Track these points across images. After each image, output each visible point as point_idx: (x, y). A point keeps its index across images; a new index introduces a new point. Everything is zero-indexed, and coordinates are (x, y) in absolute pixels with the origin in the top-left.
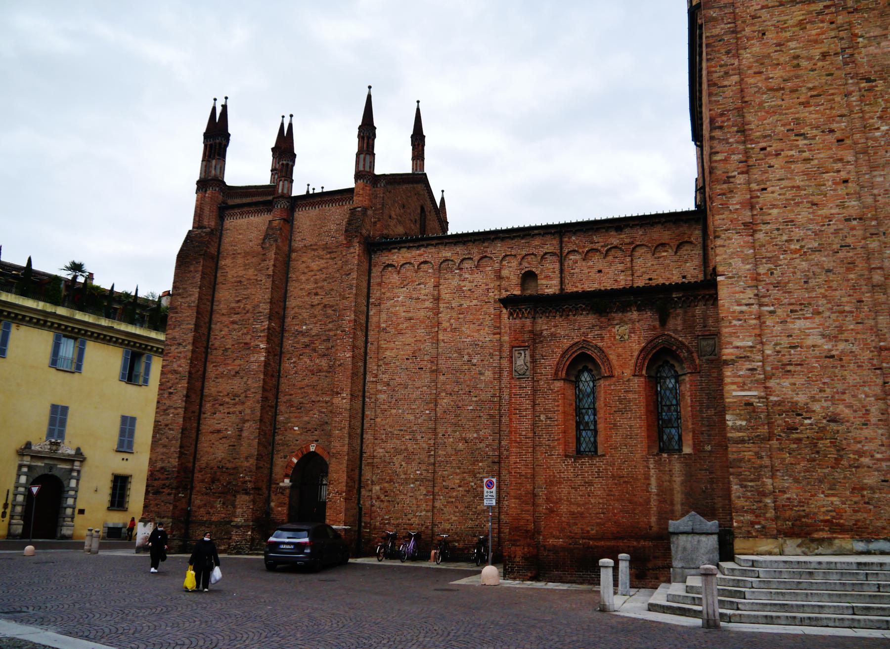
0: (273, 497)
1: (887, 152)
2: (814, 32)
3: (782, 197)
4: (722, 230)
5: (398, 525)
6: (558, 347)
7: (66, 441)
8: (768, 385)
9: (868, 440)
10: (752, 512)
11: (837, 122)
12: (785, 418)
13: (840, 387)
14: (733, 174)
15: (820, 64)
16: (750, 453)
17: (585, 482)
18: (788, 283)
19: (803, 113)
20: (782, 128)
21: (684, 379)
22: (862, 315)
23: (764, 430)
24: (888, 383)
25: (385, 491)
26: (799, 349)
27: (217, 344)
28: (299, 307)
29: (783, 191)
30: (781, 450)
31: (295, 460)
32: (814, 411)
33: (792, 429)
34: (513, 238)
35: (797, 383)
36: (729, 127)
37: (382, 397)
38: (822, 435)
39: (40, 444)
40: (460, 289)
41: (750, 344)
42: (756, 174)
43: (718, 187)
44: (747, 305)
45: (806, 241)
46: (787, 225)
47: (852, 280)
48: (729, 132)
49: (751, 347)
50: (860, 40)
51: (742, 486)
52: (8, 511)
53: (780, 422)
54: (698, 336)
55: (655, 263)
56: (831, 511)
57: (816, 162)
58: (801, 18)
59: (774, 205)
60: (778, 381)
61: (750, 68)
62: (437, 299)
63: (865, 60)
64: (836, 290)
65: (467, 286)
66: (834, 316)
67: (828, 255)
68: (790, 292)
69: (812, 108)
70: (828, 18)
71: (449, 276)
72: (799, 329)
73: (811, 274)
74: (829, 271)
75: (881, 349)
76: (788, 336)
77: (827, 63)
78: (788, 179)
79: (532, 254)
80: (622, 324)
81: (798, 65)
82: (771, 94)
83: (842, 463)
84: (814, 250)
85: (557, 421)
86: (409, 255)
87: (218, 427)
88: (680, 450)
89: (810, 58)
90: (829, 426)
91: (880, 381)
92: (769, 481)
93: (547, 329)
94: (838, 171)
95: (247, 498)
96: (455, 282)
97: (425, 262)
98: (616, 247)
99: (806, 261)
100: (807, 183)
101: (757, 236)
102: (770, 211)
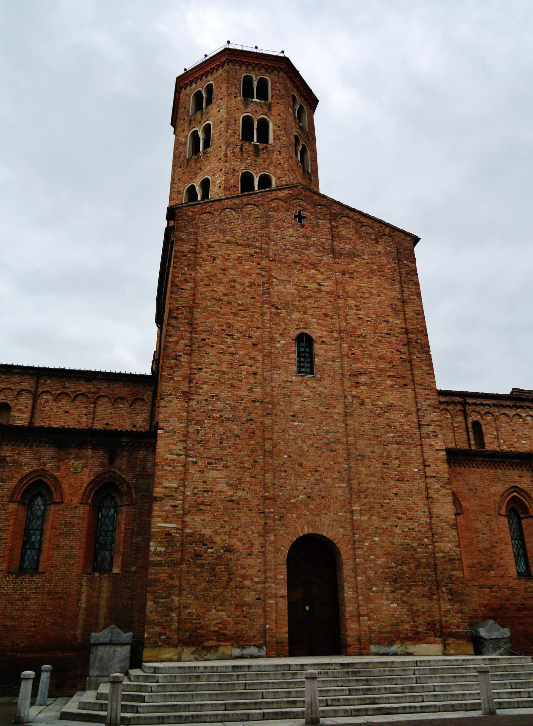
1: (282, 358)
2: (247, 267)
3: (212, 377)
4: (166, 395)
6: (18, 473)
8: (185, 519)
9: (251, 567)
10: (160, 624)
11: (254, 332)
12: (194, 547)
13: (236, 524)
14: (180, 354)
15: (248, 289)
16: (165, 575)
17: (23, 597)
18: (208, 441)
19: (233, 320)
20: (218, 328)
21: (122, 510)
22: (256, 472)
23: (177, 556)
24: (267, 524)
26: (210, 493)
29: (213, 373)
30: (188, 572)
32: (216, 543)
33: (198, 556)
35: (206, 519)
36: (182, 318)
38: (219, 562)
41: (175, 485)
42: (196, 357)
43: (168, 361)
44: (177, 455)
45: (224, 412)
46: (213, 398)
47: (252, 445)
48: (182, 323)
49: (176, 488)
50: (274, 280)
51: (156, 602)
53: (190, 550)
54: (138, 475)
55: (113, 412)
56: (219, 623)
57: (237, 356)
58: (240, 255)
59: (206, 382)
60: (192, 517)
61: (202, 280)
63: (276, 294)
64: (241, 451)
66: (237, 470)
67: (237, 425)
68: (209, 449)
69: (239, 318)
70: (256, 260)
72: (212, 478)
73: (225, 437)
74: (237, 436)
75: (266, 498)
76: (204, 482)
77: (253, 290)
78: (217, 365)
79: (10, 389)
80: (78, 459)
81: (234, 287)
82: (214, 302)
83: (231, 584)
84: (229, 420)
85: (5, 539)
88: (110, 570)
89: (242, 284)
90: (225, 554)
91: (262, 522)
92: (176, 598)
93: (10, 456)
94: (251, 366)
98: (83, 394)
99: (223, 427)
100: (230, 370)
101: (191, 403)
102: (203, 386)
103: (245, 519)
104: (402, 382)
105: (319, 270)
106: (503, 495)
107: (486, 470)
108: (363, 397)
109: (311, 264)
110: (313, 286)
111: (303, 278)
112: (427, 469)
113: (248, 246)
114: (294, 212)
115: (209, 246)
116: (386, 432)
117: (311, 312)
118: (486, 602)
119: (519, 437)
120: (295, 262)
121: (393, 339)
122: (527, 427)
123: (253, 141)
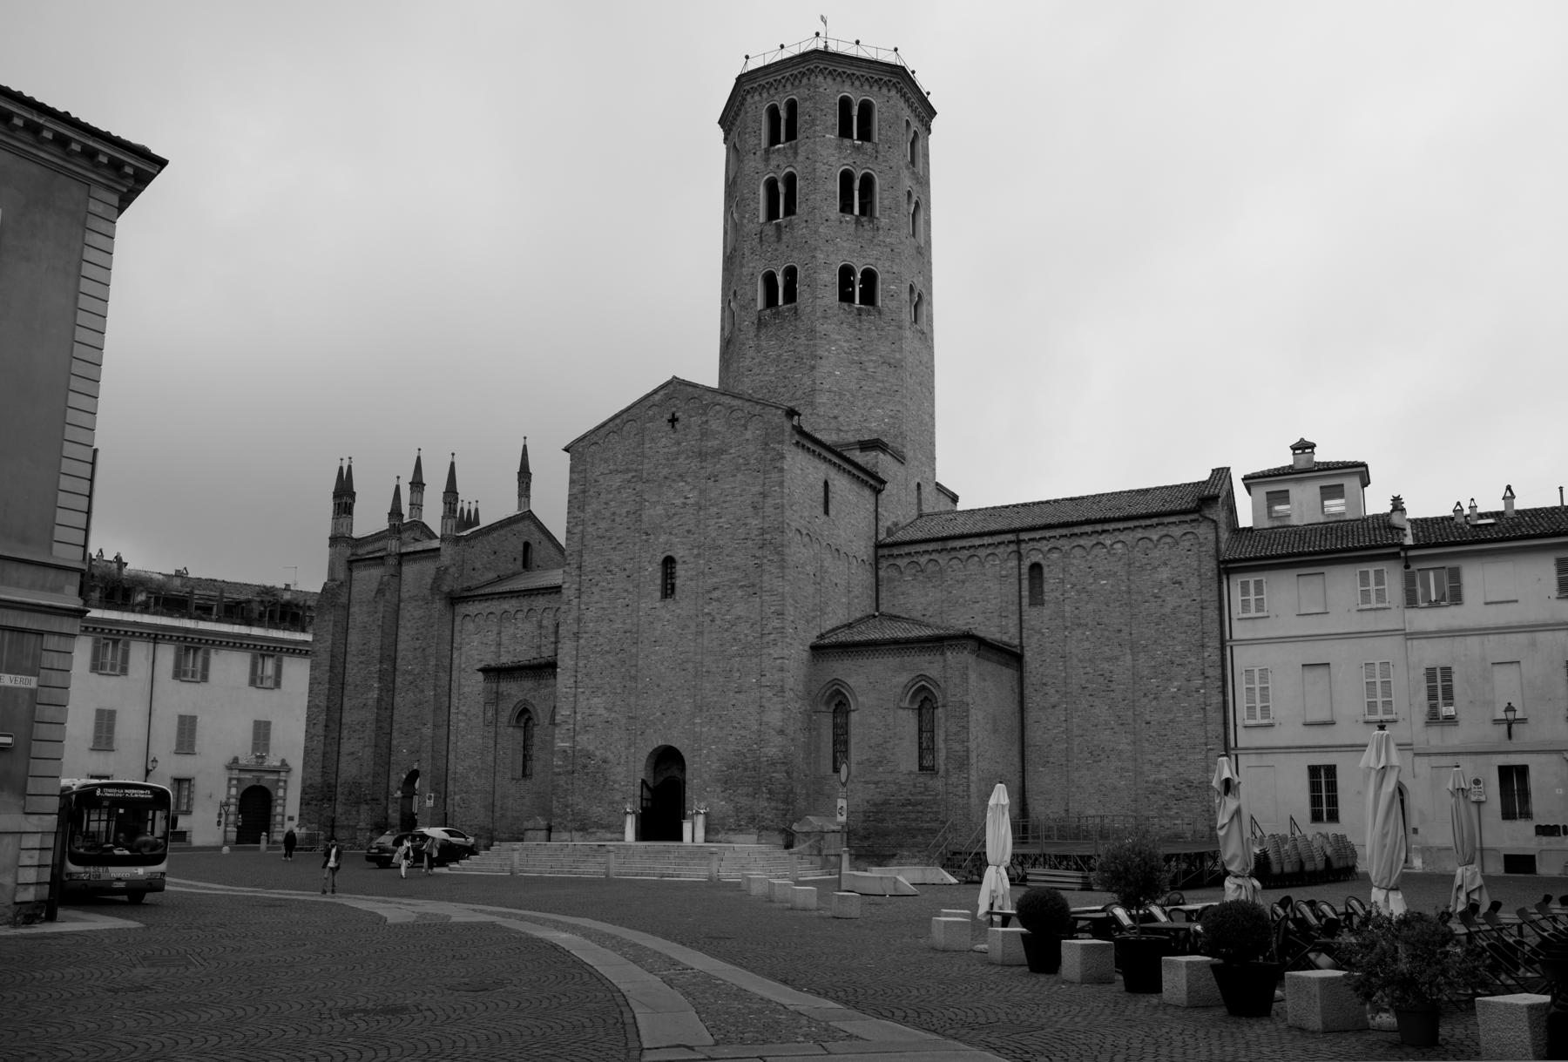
0: (390, 805)
2: (624, 495)
5: (471, 826)
7: (271, 753)
15: (625, 520)
23: (570, 768)
25: (463, 800)
27: (350, 680)
31: (404, 776)
33: (585, 767)
37: (462, 724)
39: (247, 758)
40: (514, 636)
42: (584, 598)
52: (223, 820)
62: (499, 645)
65: (520, 633)
70: (633, 485)
71: (507, 625)
74: (612, 666)
81: (613, 520)
84: (609, 652)
87: (353, 750)
89: (620, 516)
97: (491, 613)
104: (751, 590)
106: (906, 686)
108: (714, 613)
109: (680, 476)
110: (678, 502)
111: (671, 494)
112: (763, 679)
113: (628, 471)
114: (668, 416)
115: (596, 481)
116: (732, 646)
117: (675, 531)
118: (868, 798)
121: (750, 543)
122: (1114, 559)
123: (778, 218)
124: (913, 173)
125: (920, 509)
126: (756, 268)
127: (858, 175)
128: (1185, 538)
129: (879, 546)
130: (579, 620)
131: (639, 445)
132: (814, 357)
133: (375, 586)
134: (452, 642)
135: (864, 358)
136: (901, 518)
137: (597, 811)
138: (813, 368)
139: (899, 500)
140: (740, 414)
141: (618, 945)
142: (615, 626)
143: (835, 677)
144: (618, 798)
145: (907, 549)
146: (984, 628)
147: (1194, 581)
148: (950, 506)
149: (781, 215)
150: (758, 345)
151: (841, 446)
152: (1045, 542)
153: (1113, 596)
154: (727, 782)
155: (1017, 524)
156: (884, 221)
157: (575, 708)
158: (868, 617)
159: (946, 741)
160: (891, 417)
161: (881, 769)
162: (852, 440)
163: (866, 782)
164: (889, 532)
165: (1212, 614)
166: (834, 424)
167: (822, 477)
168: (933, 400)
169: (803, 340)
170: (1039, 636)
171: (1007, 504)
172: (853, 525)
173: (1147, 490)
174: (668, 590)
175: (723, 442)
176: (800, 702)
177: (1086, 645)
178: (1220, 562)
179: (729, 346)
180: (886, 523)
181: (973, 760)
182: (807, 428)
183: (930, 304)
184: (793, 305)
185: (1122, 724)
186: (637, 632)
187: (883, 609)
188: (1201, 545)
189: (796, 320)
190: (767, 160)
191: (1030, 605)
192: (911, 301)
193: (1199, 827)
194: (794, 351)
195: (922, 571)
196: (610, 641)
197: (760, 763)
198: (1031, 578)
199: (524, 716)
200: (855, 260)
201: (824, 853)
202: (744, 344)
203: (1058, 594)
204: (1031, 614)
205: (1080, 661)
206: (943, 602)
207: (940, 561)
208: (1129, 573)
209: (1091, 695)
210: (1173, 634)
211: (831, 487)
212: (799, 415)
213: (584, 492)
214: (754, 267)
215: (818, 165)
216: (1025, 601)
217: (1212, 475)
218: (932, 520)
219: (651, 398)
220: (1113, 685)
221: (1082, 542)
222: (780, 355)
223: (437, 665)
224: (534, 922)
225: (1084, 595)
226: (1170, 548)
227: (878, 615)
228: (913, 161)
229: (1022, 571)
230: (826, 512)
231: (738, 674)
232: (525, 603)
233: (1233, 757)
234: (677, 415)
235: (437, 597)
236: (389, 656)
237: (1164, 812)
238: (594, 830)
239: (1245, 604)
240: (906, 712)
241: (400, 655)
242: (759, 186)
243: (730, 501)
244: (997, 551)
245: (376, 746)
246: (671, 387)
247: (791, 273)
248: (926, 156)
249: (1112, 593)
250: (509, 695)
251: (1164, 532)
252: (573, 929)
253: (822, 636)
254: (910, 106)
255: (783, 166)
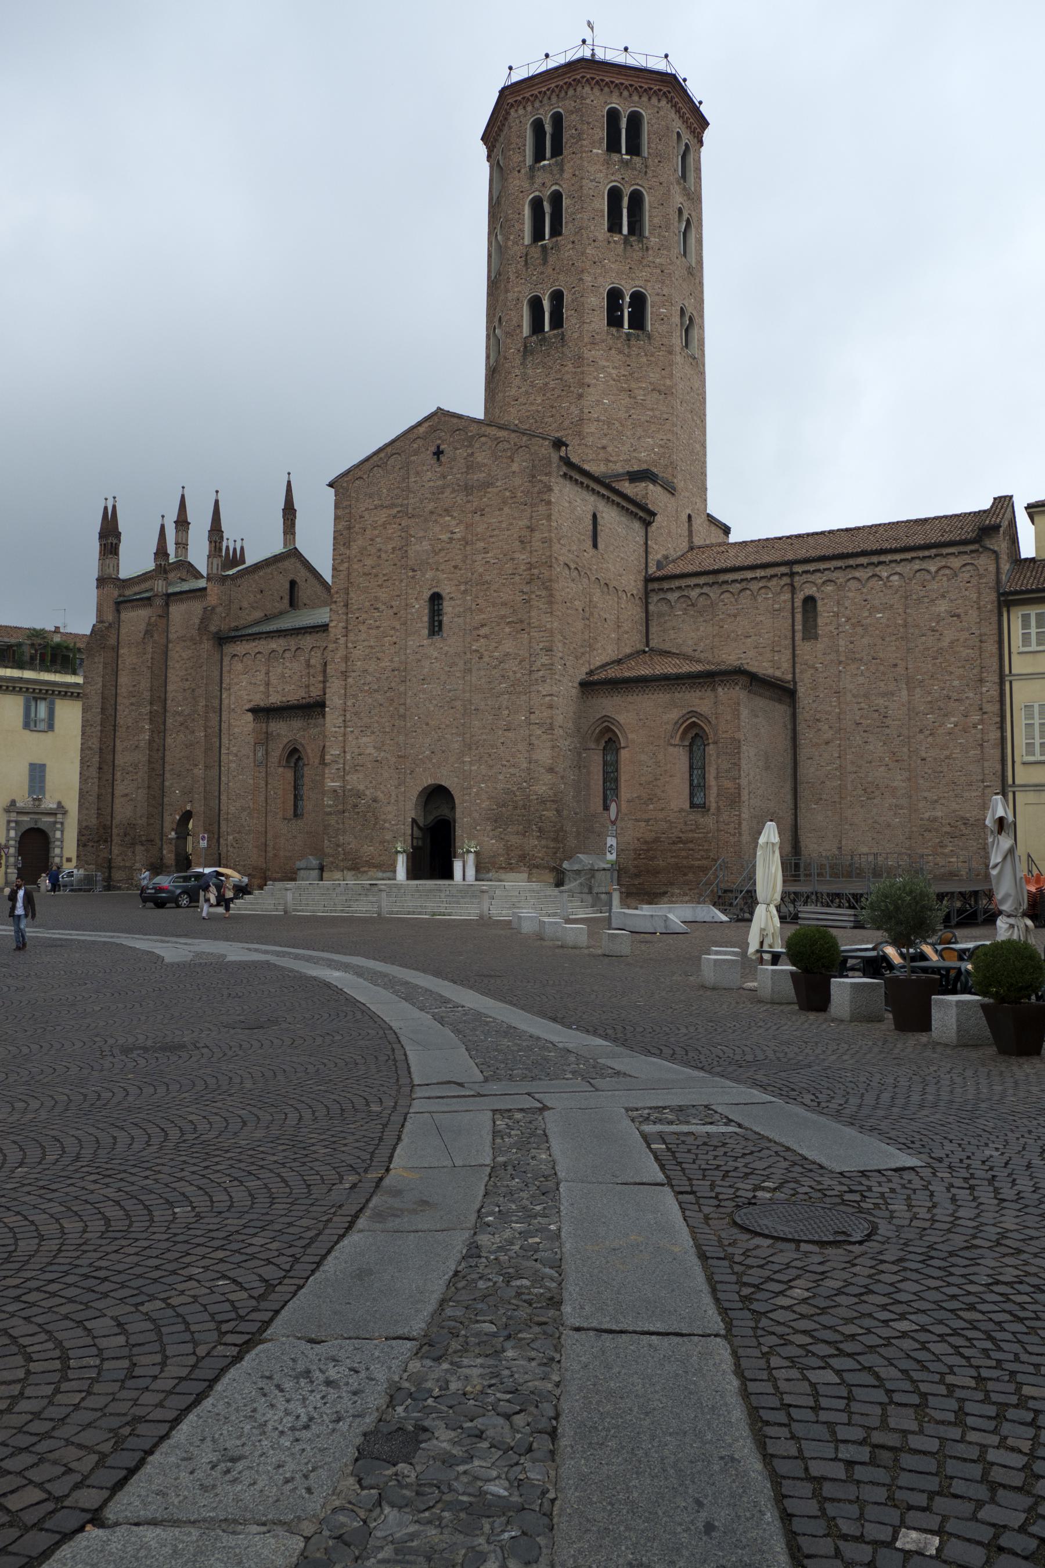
0: (165, 846)
7: (47, 796)
23: (340, 807)
27: (122, 722)
28: (176, 691)
33: (355, 806)
34: (317, 632)
39: (24, 801)
40: (283, 676)
42: (352, 637)
62: (268, 684)
65: (288, 673)
70: (398, 520)
75: (399, 757)
81: (379, 557)
84: (376, 691)
86: (247, 647)
87: (126, 791)
89: (386, 552)
95: (143, 848)
96: (279, 670)
97: (259, 653)
103: (386, 775)
104: (519, 626)
105: (451, 516)
106: (676, 723)
107: (661, 695)
109: (446, 510)
111: (437, 529)
113: (393, 506)
114: (433, 449)
115: (361, 517)
116: (500, 683)
119: (873, 610)
120: (432, 513)
121: (517, 578)
123: (544, 239)
124: (685, 189)
125: (691, 541)
126: (521, 292)
127: (627, 191)
128: (964, 569)
129: (648, 580)
130: (346, 659)
131: (404, 479)
132: (582, 384)
133: (143, 627)
134: (221, 683)
135: (633, 385)
136: (672, 552)
137: (368, 850)
138: (580, 396)
139: (670, 532)
140: (506, 446)
141: (390, 983)
142: (383, 664)
143: (604, 714)
144: (388, 836)
145: (677, 583)
146: (756, 664)
147: (973, 615)
148: (721, 538)
149: (547, 237)
150: (525, 374)
151: (610, 477)
152: (819, 574)
153: (889, 630)
154: (497, 820)
155: (790, 556)
156: (654, 241)
157: (344, 747)
158: (638, 652)
159: (717, 778)
160: (661, 446)
161: (651, 807)
162: (621, 471)
163: (637, 820)
164: (659, 565)
165: (991, 647)
166: (602, 455)
167: (590, 508)
168: (705, 428)
169: (570, 367)
170: (812, 671)
171: (780, 535)
172: (622, 559)
173: (926, 520)
174: (436, 627)
175: (489, 475)
176: (569, 740)
177: (861, 680)
178: (1000, 595)
179: (493, 374)
180: (655, 556)
181: (745, 796)
182: (575, 460)
183: (702, 327)
184: (560, 331)
185: (897, 761)
186: (405, 670)
187: (652, 644)
188: (981, 576)
189: (563, 346)
190: (532, 178)
191: (803, 639)
192: (682, 324)
193: (974, 865)
194: (561, 379)
195: (693, 605)
196: (378, 679)
197: (530, 801)
198: (805, 611)
199: (294, 756)
200: (623, 283)
201: (595, 890)
202: (510, 373)
203: (832, 628)
204: (804, 649)
205: (854, 696)
206: (714, 636)
207: (711, 595)
208: (906, 607)
209: (865, 731)
210: (949, 668)
211: (599, 519)
212: (567, 446)
213: (349, 528)
214: (520, 292)
215: (585, 182)
216: (799, 636)
217: (993, 504)
218: (703, 553)
219: (415, 431)
220: (888, 721)
221: (857, 574)
222: (546, 384)
223: (207, 706)
224: (307, 961)
225: (859, 630)
226: (949, 580)
227: (648, 651)
228: (684, 176)
229: (796, 605)
230: (595, 546)
231: (507, 712)
232: (292, 643)
233: (1010, 795)
234: (442, 447)
235: (205, 637)
236: (159, 698)
237: (940, 850)
238: (365, 869)
239: (1026, 638)
240: (676, 749)
241: (170, 695)
242: (523, 206)
243: (497, 536)
244: (769, 584)
245: (149, 787)
246: (436, 418)
247: (557, 297)
248: (698, 170)
249: (888, 626)
250: (278, 735)
251: (943, 564)
252: (346, 967)
253: (591, 673)
254: (681, 117)
255: (548, 184)
